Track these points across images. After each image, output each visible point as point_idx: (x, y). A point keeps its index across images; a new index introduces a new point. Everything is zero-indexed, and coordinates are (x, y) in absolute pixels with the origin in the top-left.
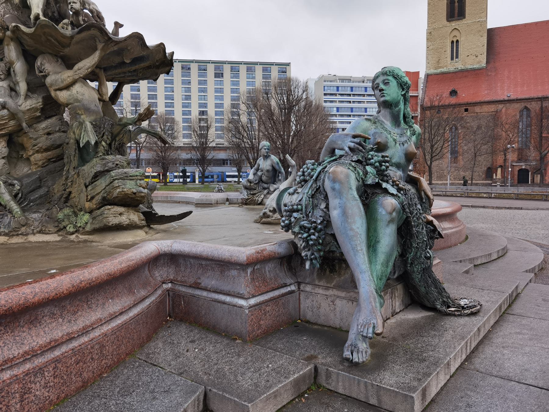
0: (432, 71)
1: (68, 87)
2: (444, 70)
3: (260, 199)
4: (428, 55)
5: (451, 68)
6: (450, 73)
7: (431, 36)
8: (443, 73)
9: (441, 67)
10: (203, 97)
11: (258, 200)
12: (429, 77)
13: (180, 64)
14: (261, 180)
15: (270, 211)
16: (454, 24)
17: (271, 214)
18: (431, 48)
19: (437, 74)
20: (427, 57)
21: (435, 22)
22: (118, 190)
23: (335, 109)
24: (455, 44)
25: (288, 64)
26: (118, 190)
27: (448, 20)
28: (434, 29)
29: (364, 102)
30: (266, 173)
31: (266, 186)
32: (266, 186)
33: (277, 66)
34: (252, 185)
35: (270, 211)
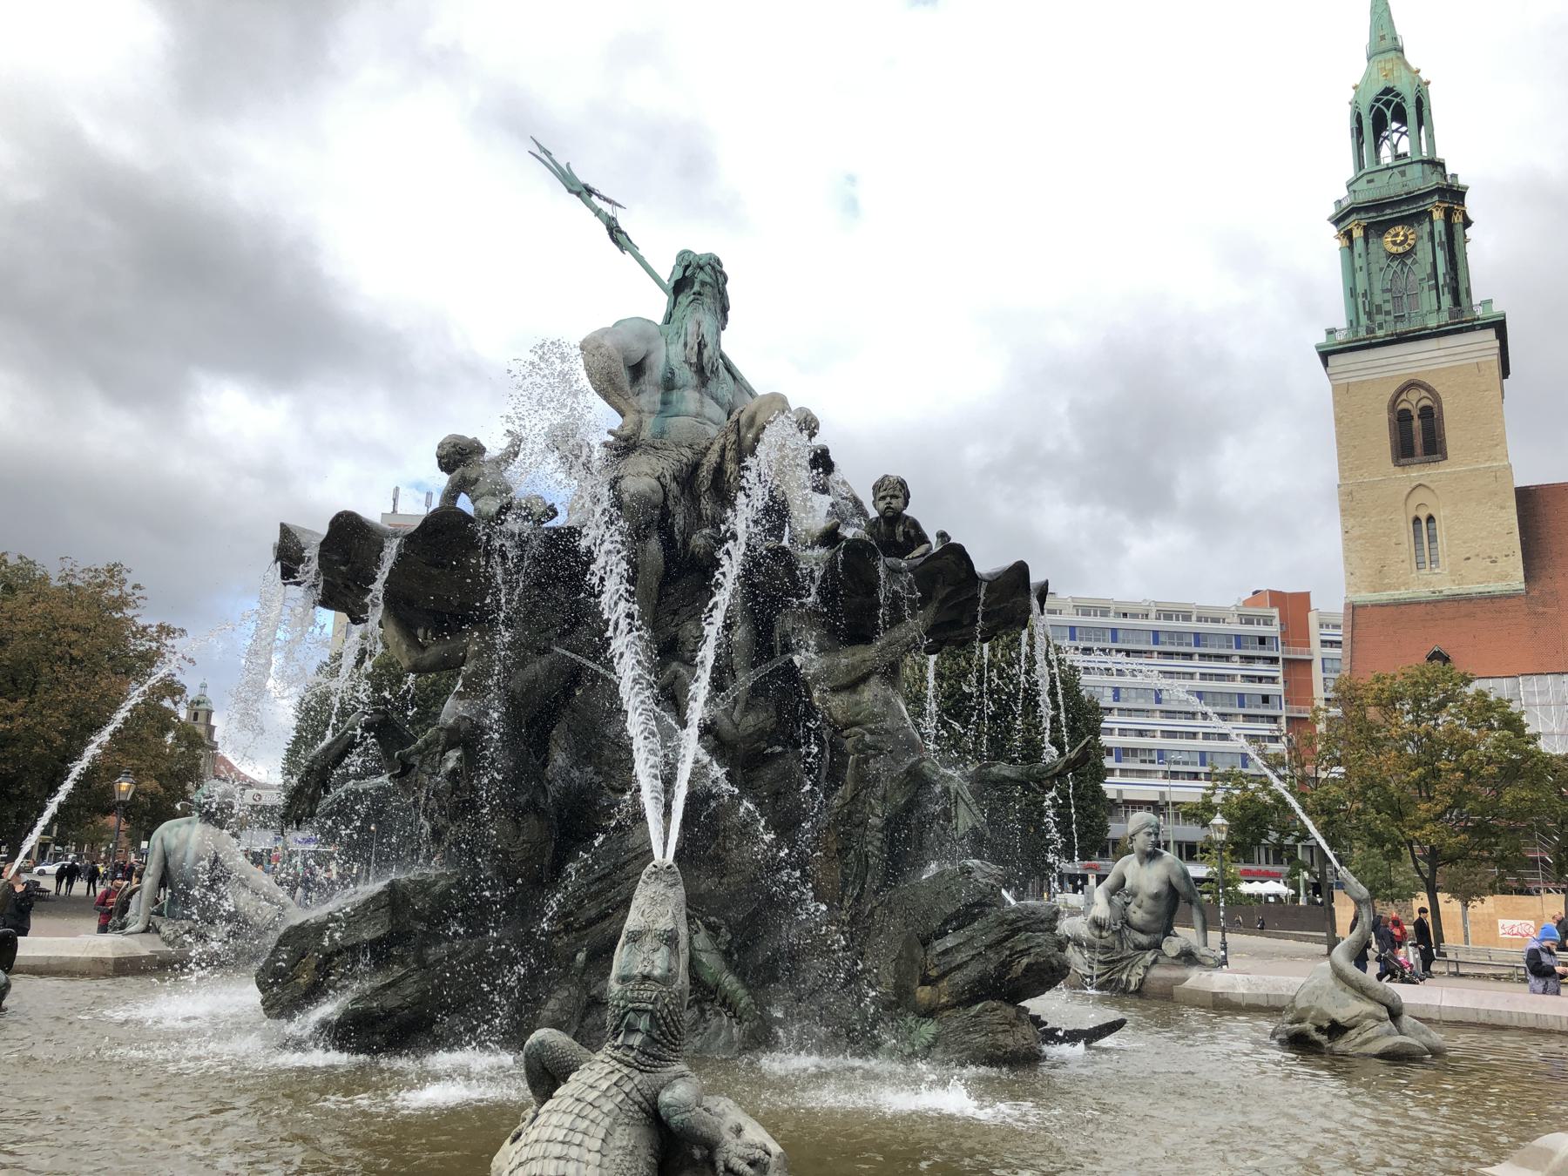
0: (1365, 596)
1: (853, 686)
3: (1134, 980)
5: (1423, 592)
6: (1419, 603)
8: (1398, 604)
9: (1389, 587)
11: (1128, 982)
14: (1127, 923)
15: (1319, 1029)
16: (1417, 473)
17: (1323, 1038)
18: (1356, 532)
20: (1346, 558)
22: (1025, 961)
23: (1109, 693)
24: (1424, 525)
26: (1025, 961)
27: (1397, 464)
29: (1192, 675)
30: (1147, 903)
31: (1143, 939)
32: (1143, 939)
34: (1104, 934)
35: (1319, 1029)
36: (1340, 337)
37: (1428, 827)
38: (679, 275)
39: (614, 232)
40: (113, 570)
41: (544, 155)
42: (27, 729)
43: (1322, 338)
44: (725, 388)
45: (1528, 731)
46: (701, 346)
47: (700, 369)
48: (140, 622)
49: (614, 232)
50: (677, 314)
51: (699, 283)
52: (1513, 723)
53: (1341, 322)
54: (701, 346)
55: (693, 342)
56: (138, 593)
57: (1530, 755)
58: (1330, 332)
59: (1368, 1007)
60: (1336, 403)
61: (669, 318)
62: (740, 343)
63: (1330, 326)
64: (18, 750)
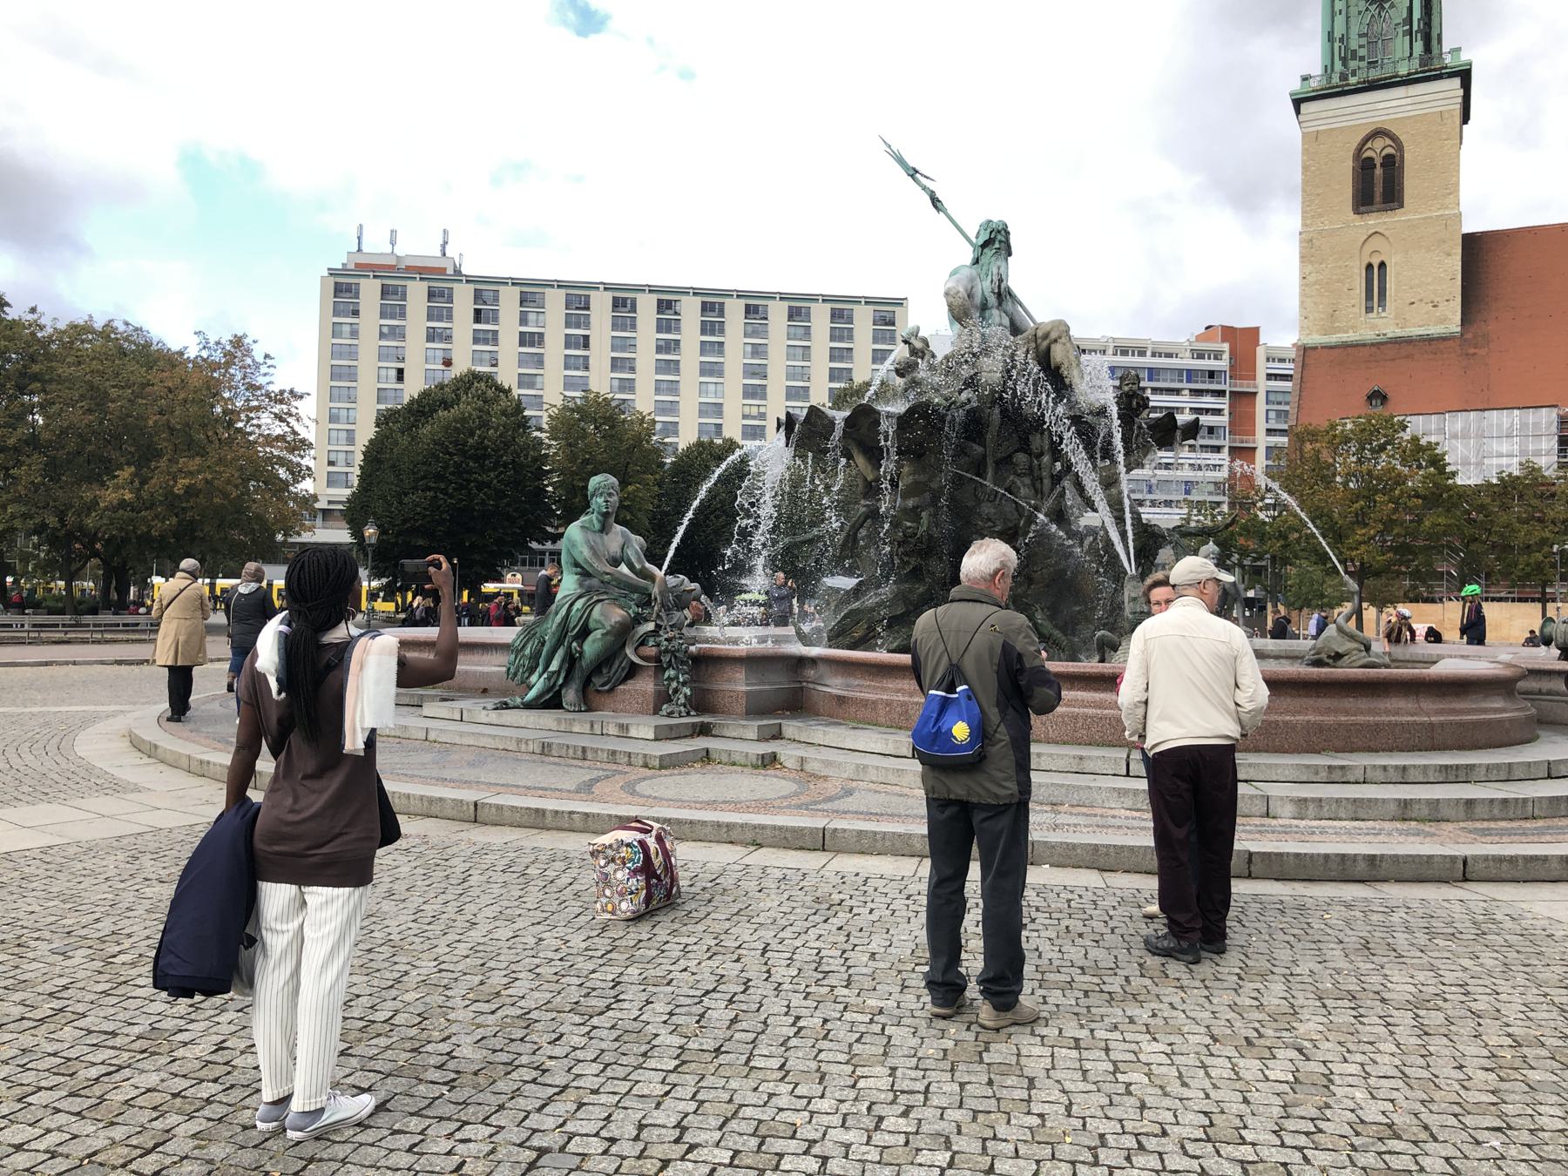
0: (1317, 339)
2: (1350, 336)
4: (1304, 295)
5: (1368, 335)
6: (1364, 345)
7: (1311, 250)
8: (1345, 346)
9: (1340, 330)
10: (712, 387)
12: (1309, 353)
13: (609, 295)
16: (1374, 221)
18: (1312, 278)
19: (1331, 348)
20: (1302, 303)
21: (1321, 215)
24: (1375, 275)
25: (899, 303)
27: (1357, 211)
28: (1320, 232)
33: (872, 307)
36: (1314, 84)
37: (1363, 548)
38: (984, 237)
39: (936, 202)
40: (238, 342)
41: (901, 161)
42: (207, 481)
43: (1296, 85)
44: (1008, 305)
45: (1448, 469)
46: (1001, 281)
47: (999, 295)
48: (275, 388)
49: (936, 202)
50: (983, 260)
51: (996, 241)
52: (1437, 462)
53: (1317, 70)
54: (1001, 281)
55: (995, 278)
56: (269, 362)
57: (1450, 488)
58: (1305, 79)
59: (1356, 645)
60: (1305, 151)
61: (976, 261)
62: (1021, 276)
63: (1305, 73)
64: (202, 500)
